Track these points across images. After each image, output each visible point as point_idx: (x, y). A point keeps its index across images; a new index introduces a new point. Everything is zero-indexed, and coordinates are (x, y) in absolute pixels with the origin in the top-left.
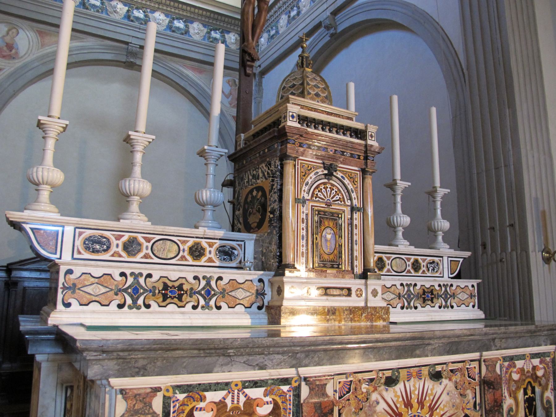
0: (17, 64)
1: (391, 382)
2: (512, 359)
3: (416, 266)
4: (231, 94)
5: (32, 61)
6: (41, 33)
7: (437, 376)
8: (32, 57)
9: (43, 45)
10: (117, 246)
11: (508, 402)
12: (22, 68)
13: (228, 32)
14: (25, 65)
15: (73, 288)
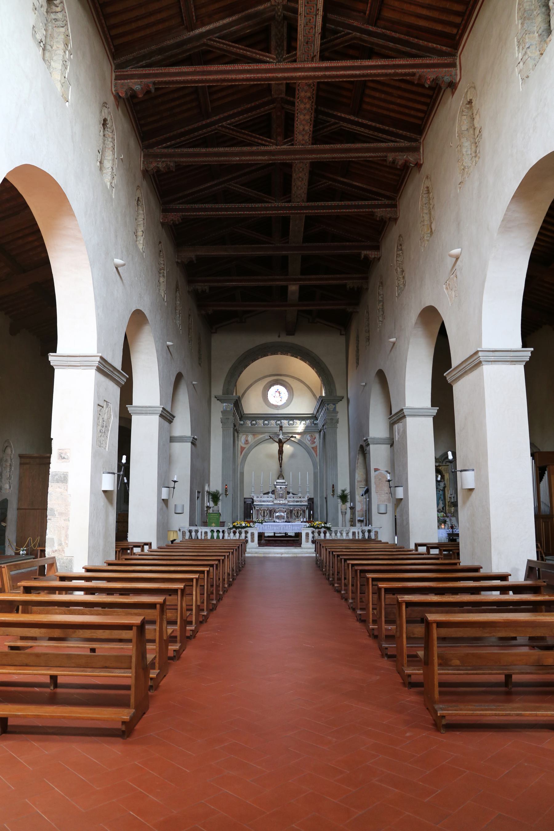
0: (249, 445)
1: (278, 508)
2: (295, 508)
3: (300, 498)
4: (310, 440)
5: (252, 444)
6: (254, 435)
7: (284, 509)
8: (252, 442)
9: (255, 438)
10: (260, 497)
11: (294, 512)
12: (250, 446)
13: (307, 420)
14: (251, 445)
15: (255, 501)
